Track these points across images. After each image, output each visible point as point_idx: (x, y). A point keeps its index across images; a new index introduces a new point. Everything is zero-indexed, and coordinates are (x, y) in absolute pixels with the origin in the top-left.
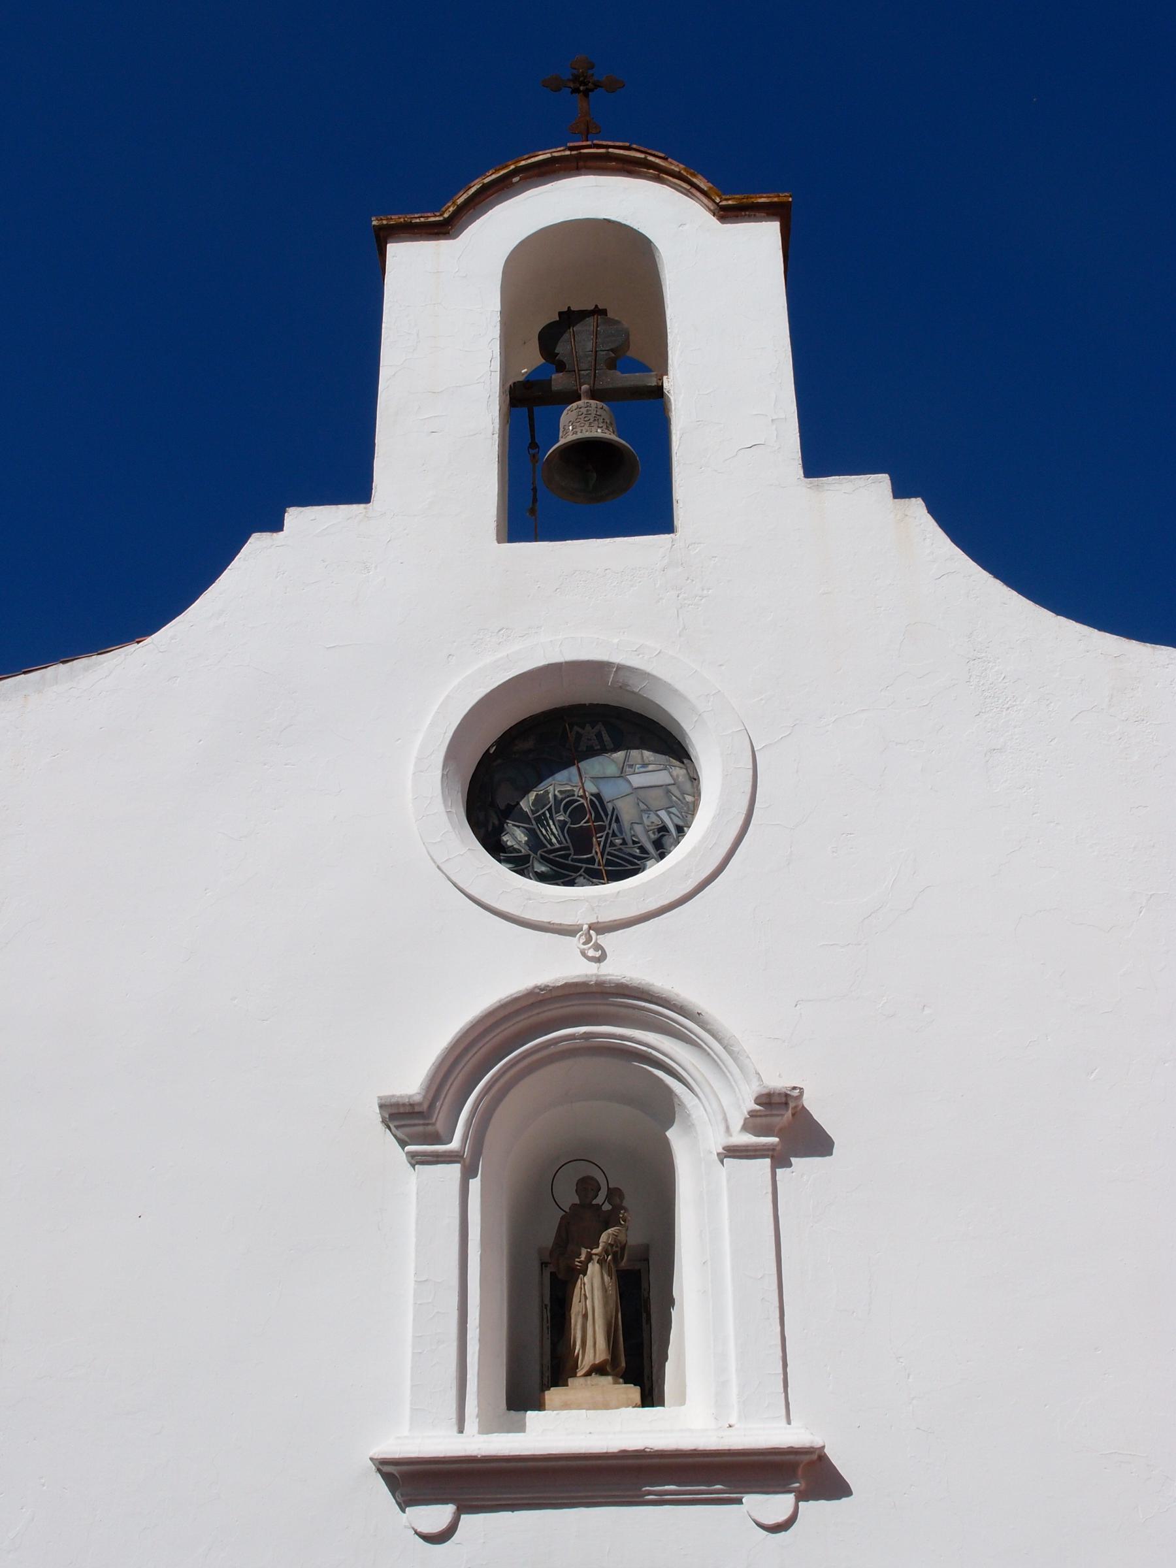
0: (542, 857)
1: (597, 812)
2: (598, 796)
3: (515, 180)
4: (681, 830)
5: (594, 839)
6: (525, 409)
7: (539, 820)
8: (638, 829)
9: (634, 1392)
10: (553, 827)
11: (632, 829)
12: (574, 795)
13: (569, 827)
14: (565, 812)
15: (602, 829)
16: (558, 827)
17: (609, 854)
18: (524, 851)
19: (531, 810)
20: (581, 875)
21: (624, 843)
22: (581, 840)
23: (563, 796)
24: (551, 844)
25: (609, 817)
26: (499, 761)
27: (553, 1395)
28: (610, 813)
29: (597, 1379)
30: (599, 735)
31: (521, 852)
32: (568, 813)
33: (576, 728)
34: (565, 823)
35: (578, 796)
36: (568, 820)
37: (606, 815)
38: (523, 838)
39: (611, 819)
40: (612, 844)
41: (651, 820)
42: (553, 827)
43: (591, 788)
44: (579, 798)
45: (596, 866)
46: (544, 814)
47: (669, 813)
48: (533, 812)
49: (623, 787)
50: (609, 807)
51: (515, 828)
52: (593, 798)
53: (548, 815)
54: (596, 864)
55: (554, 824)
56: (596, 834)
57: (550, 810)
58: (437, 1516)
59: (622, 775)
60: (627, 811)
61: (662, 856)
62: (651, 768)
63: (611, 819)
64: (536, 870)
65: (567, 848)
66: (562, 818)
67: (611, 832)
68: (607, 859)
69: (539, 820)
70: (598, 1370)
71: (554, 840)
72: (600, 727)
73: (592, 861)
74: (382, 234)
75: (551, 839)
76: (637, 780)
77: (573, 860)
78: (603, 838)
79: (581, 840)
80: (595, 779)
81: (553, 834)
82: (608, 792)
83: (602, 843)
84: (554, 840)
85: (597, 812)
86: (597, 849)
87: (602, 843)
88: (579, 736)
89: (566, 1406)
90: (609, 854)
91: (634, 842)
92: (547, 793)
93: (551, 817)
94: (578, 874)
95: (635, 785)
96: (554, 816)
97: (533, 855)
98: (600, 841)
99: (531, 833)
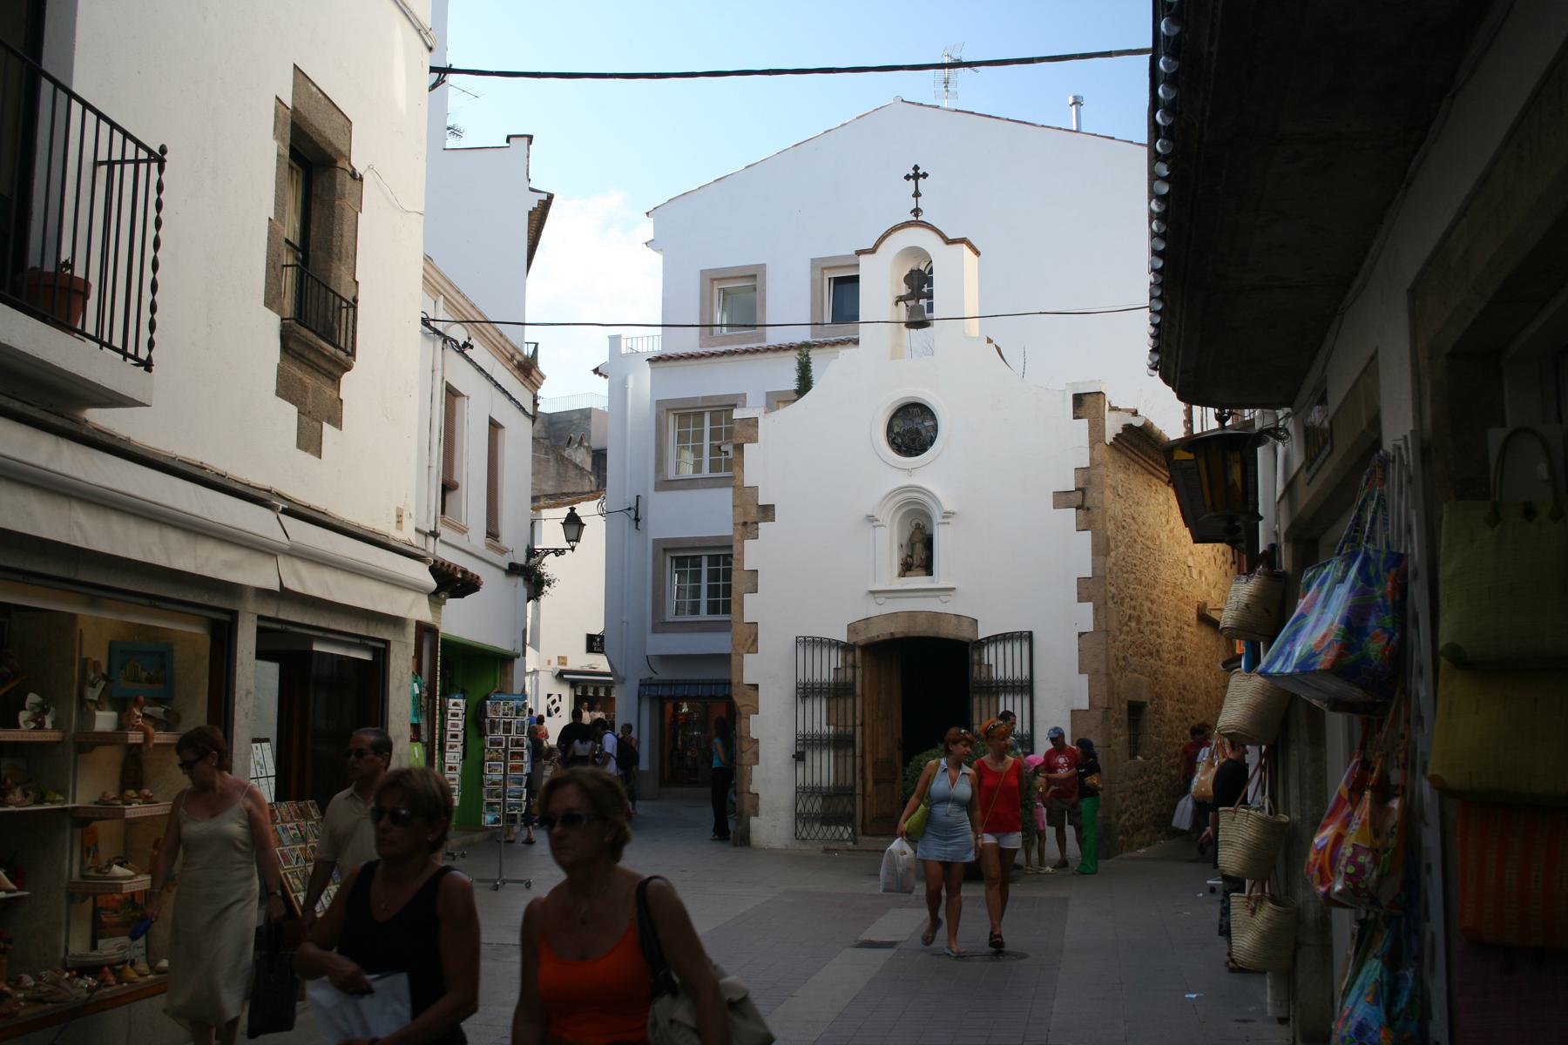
4: (936, 437)
7: (904, 436)
9: (924, 573)
22: (913, 441)
27: (907, 573)
29: (919, 569)
38: (900, 440)
41: (929, 434)
58: (881, 601)
60: (923, 432)
61: (932, 445)
70: (919, 566)
76: (926, 424)
79: (913, 441)
80: (916, 424)
89: (911, 576)
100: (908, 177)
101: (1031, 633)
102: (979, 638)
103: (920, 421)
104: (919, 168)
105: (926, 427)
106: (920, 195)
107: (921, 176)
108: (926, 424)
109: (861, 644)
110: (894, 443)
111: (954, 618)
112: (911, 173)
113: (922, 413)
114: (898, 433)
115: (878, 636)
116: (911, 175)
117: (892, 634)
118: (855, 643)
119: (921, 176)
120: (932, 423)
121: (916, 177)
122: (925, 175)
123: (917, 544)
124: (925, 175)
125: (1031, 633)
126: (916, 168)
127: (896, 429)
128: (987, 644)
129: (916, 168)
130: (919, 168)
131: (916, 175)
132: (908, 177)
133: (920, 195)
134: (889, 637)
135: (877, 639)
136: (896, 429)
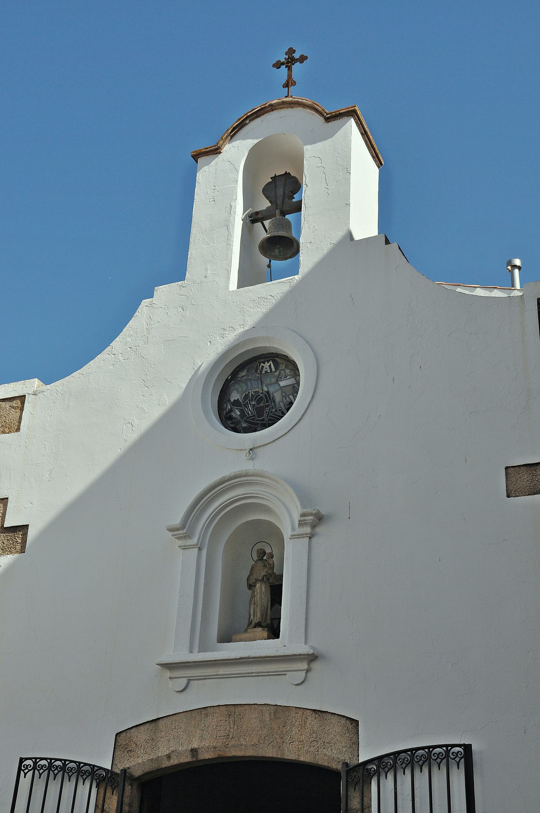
0: (245, 421)
1: (267, 399)
2: (268, 392)
3: (247, 122)
5: (265, 411)
6: (260, 224)
7: (246, 405)
8: (282, 404)
10: (250, 407)
11: (279, 404)
12: (259, 393)
13: (256, 407)
14: (255, 401)
15: (268, 406)
16: (252, 407)
17: (270, 416)
18: (239, 418)
19: (243, 401)
20: (259, 426)
21: (276, 411)
22: (260, 411)
23: (255, 394)
24: (248, 414)
25: (271, 401)
26: (233, 382)
28: (271, 399)
30: (270, 366)
31: (237, 419)
32: (256, 401)
33: (262, 364)
34: (254, 405)
35: (261, 393)
36: (256, 404)
37: (270, 398)
38: (238, 413)
39: (272, 401)
40: (272, 412)
42: (250, 407)
43: (265, 389)
44: (260, 394)
45: (265, 422)
46: (247, 402)
47: (293, 396)
48: (243, 402)
49: (277, 387)
50: (272, 395)
51: (236, 409)
52: (266, 394)
53: (249, 402)
54: (265, 421)
55: (250, 406)
56: (266, 408)
57: (249, 400)
59: (277, 382)
60: (278, 397)
62: (288, 378)
63: (272, 401)
64: (242, 426)
65: (254, 416)
66: (254, 403)
67: (271, 406)
68: (269, 418)
69: (245, 405)
70: (258, 625)
71: (250, 413)
72: (271, 362)
73: (263, 420)
74: (195, 157)
75: (249, 413)
76: (282, 384)
77: (257, 420)
78: (268, 410)
81: (250, 410)
82: (271, 390)
83: (268, 412)
84: (250, 413)
85: (267, 399)
86: (265, 414)
87: (268, 412)
88: (263, 367)
90: (270, 416)
91: (280, 410)
92: (249, 393)
93: (250, 404)
94: (258, 426)
95: (282, 385)
96: (251, 403)
97: (242, 420)
98: (267, 411)
99: (242, 411)
100: (278, 65)
101: (468, 748)
102: (362, 760)
103: (273, 380)
104: (294, 51)
105: (281, 388)
106: (294, 83)
107: (297, 60)
108: (282, 384)
109: (137, 773)
110: (231, 418)
111: (312, 722)
112: (283, 58)
113: (276, 369)
114: (236, 403)
115: (169, 757)
116: (283, 60)
117: (194, 751)
118: (124, 771)
119: (297, 60)
120: (291, 381)
121: (290, 62)
122: (303, 59)
123: (258, 585)
124: (303, 59)
125: (468, 748)
126: (291, 51)
127: (235, 396)
128: (377, 773)
129: (291, 51)
130: (294, 51)
131: (290, 62)
132: (278, 65)
133: (294, 83)
134: (187, 759)
135: (166, 764)
136: (235, 396)
